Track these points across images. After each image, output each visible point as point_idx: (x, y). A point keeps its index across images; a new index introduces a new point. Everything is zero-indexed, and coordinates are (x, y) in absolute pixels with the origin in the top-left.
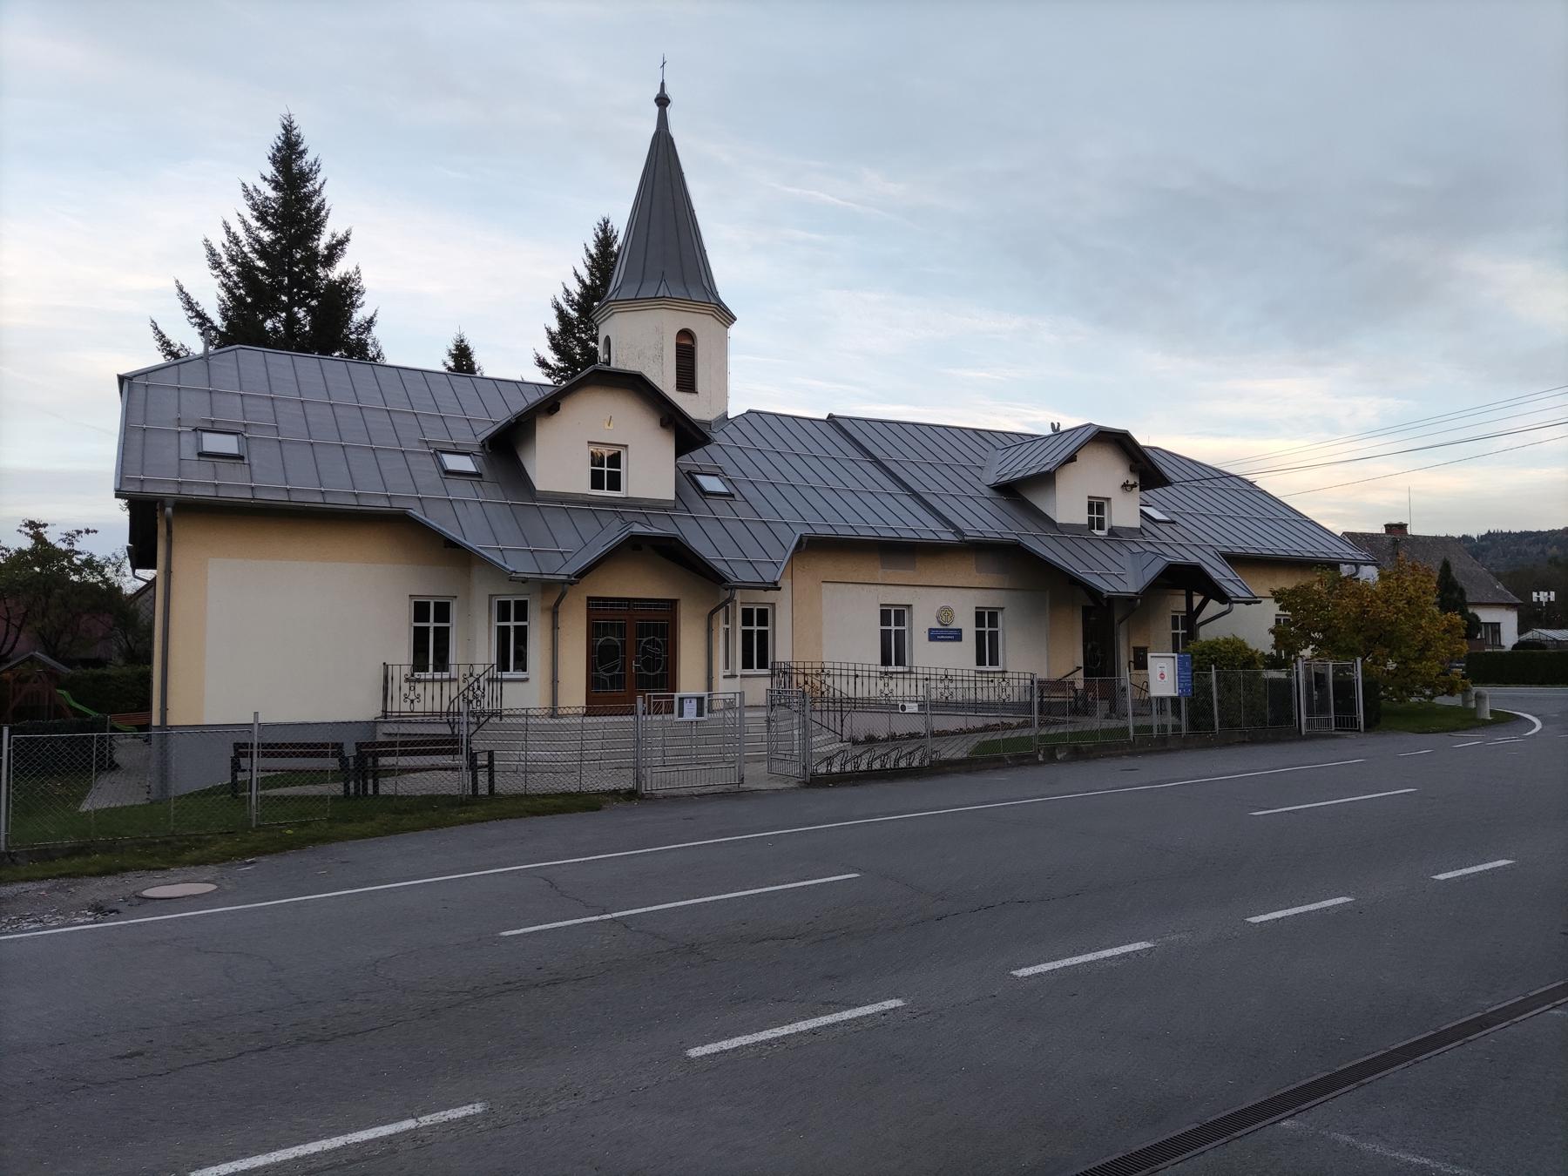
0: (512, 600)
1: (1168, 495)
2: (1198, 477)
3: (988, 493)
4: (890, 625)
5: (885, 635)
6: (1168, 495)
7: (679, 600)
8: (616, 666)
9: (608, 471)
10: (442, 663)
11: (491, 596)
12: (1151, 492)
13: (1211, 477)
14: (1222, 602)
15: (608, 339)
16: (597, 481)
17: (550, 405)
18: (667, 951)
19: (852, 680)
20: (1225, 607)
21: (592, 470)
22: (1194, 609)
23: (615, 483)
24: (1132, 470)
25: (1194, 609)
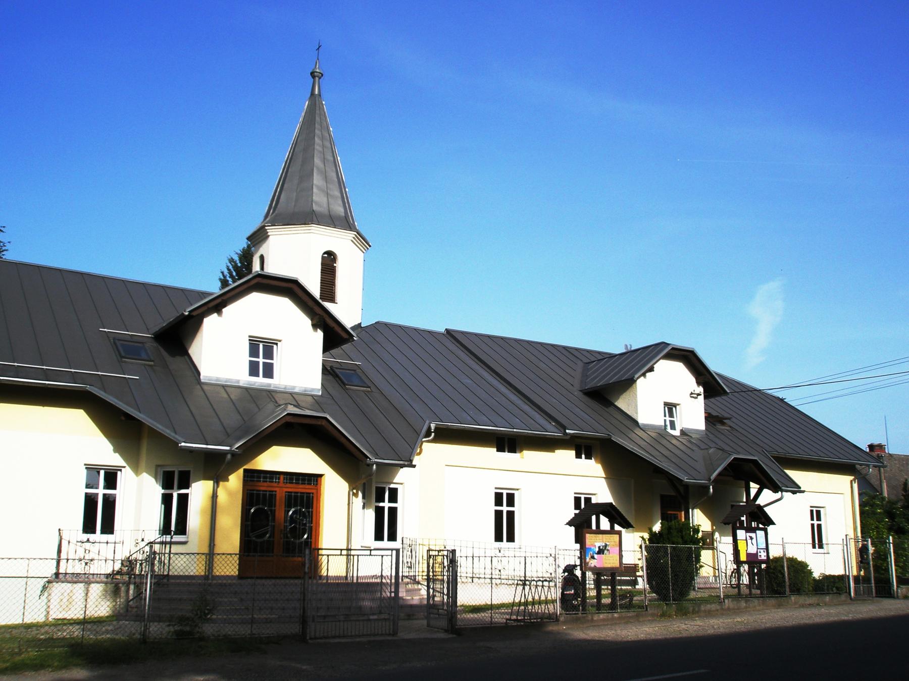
0: (177, 470)
1: (725, 403)
2: (743, 394)
3: (580, 395)
4: (502, 506)
5: (498, 514)
6: (725, 403)
7: (321, 476)
8: (266, 533)
9: (264, 363)
10: (108, 528)
11: (158, 466)
12: (712, 400)
13: (754, 392)
14: (775, 491)
15: (262, 258)
16: (254, 370)
17: (217, 305)
18: (601, 625)
19: (470, 559)
20: (779, 495)
21: (250, 361)
22: (751, 499)
23: (269, 372)
24: (699, 383)
25: (751, 499)
